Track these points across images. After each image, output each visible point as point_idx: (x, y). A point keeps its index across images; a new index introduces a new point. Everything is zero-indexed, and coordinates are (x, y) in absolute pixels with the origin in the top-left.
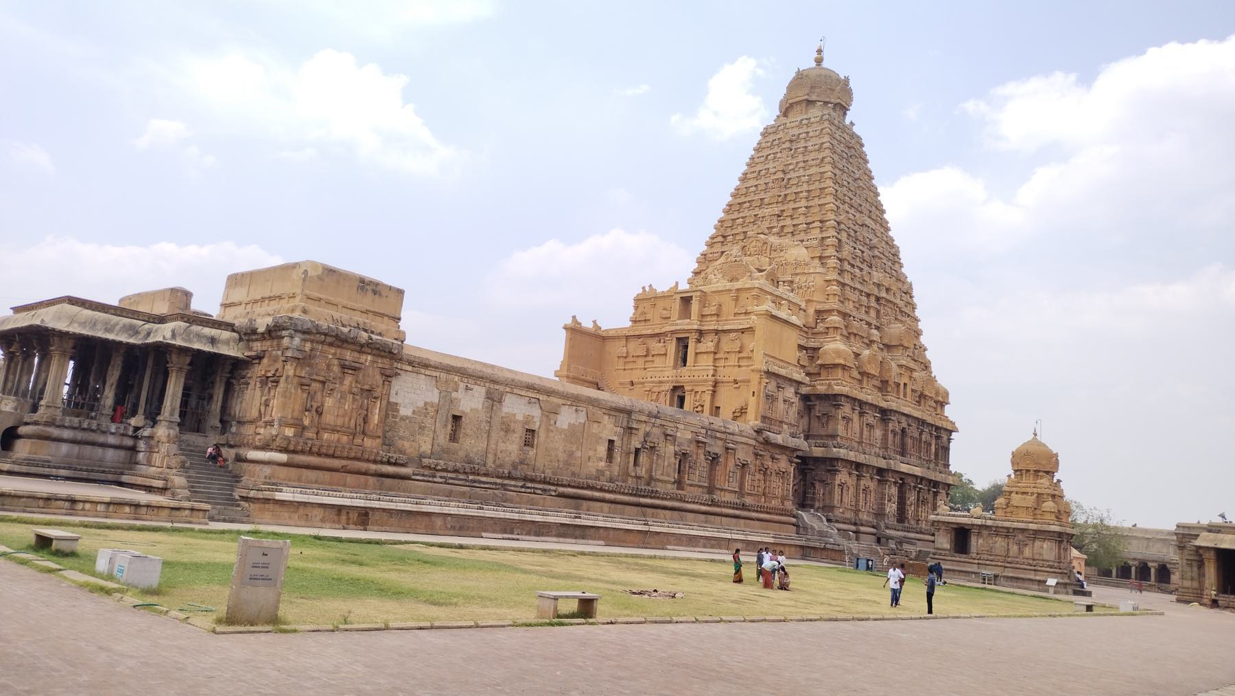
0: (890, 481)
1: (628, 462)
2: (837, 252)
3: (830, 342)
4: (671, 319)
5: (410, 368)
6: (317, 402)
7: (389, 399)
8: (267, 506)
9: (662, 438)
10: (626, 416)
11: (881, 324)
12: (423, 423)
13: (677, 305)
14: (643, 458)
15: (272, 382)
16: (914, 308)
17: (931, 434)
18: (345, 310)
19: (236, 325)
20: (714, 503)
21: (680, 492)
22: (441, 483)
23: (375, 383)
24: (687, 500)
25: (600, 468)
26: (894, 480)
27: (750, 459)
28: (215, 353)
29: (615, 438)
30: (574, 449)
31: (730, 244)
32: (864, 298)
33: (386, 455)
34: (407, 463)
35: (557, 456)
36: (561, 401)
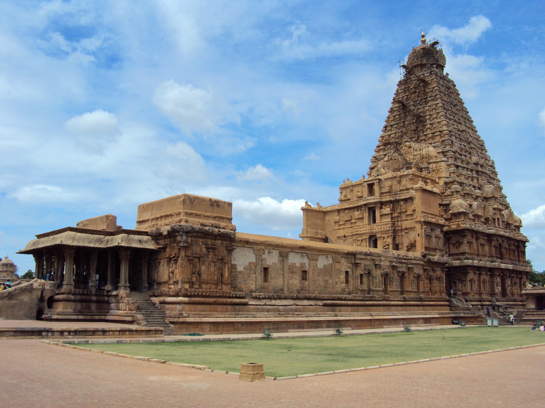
0: (496, 275)
2: (452, 148)
3: (455, 200)
4: (364, 197)
5: (239, 245)
6: (197, 269)
8: (183, 325)
9: (374, 267)
10: (353, 257)
11: (480, 186)
12: (249, 274)
13: (366, 190)
14: (365, 279)
15: (174, 260)
16: (496, 175)
17: (515, 245)
18: (204, 218)
19: (149, 232)
20: (405, 300)
21: (386, 295)
23: (224, 255)
24: (390, 299)
26: (498, 274)
27: (421, 272)
28: (143, 249)
29: (349, 270)
30: (328, 278)
32: (469, 172)
33: (234, 293)
35: (319, 284)
36: (317, 253)
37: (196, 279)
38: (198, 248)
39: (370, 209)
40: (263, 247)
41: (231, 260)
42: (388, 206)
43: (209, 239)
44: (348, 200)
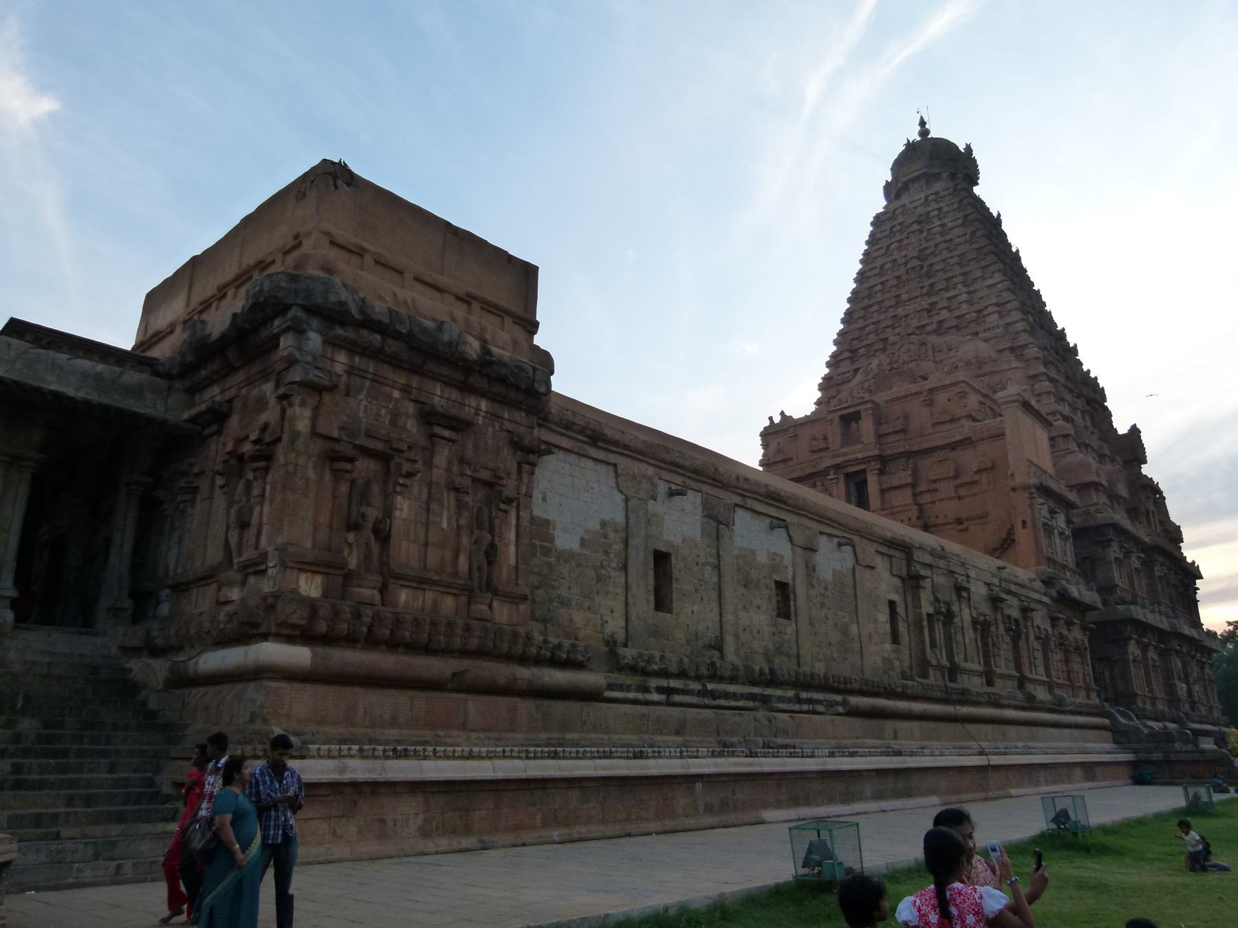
1: (923, 642)
5: (565, 443)
7: (532, 512)
9: (954, 594)
10: (902, 555)
12: (602, 567)
13: (834, 433)
18: (419, 287)
20: (1031, 703)
22: (658, 703)
25: (886, 655)
27: (1049, 629)
29: (895, 597)
30: (847, 620)
31: (862, 359)
32: (1076, 399)
34: (589, 659)
37: (367, 557)
38: (383, 411)
39: (848, 476)
40: (651, 471)
41: (529, 495)
42: (902, 467)
43: (435, 378)
44: (785, 461)
